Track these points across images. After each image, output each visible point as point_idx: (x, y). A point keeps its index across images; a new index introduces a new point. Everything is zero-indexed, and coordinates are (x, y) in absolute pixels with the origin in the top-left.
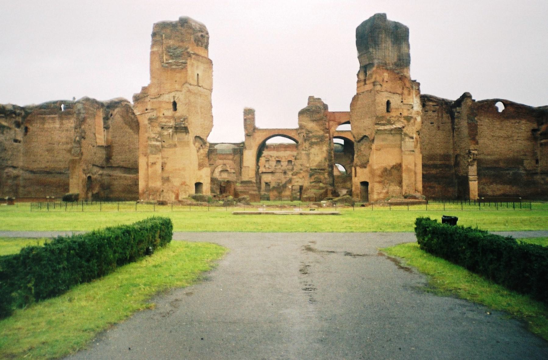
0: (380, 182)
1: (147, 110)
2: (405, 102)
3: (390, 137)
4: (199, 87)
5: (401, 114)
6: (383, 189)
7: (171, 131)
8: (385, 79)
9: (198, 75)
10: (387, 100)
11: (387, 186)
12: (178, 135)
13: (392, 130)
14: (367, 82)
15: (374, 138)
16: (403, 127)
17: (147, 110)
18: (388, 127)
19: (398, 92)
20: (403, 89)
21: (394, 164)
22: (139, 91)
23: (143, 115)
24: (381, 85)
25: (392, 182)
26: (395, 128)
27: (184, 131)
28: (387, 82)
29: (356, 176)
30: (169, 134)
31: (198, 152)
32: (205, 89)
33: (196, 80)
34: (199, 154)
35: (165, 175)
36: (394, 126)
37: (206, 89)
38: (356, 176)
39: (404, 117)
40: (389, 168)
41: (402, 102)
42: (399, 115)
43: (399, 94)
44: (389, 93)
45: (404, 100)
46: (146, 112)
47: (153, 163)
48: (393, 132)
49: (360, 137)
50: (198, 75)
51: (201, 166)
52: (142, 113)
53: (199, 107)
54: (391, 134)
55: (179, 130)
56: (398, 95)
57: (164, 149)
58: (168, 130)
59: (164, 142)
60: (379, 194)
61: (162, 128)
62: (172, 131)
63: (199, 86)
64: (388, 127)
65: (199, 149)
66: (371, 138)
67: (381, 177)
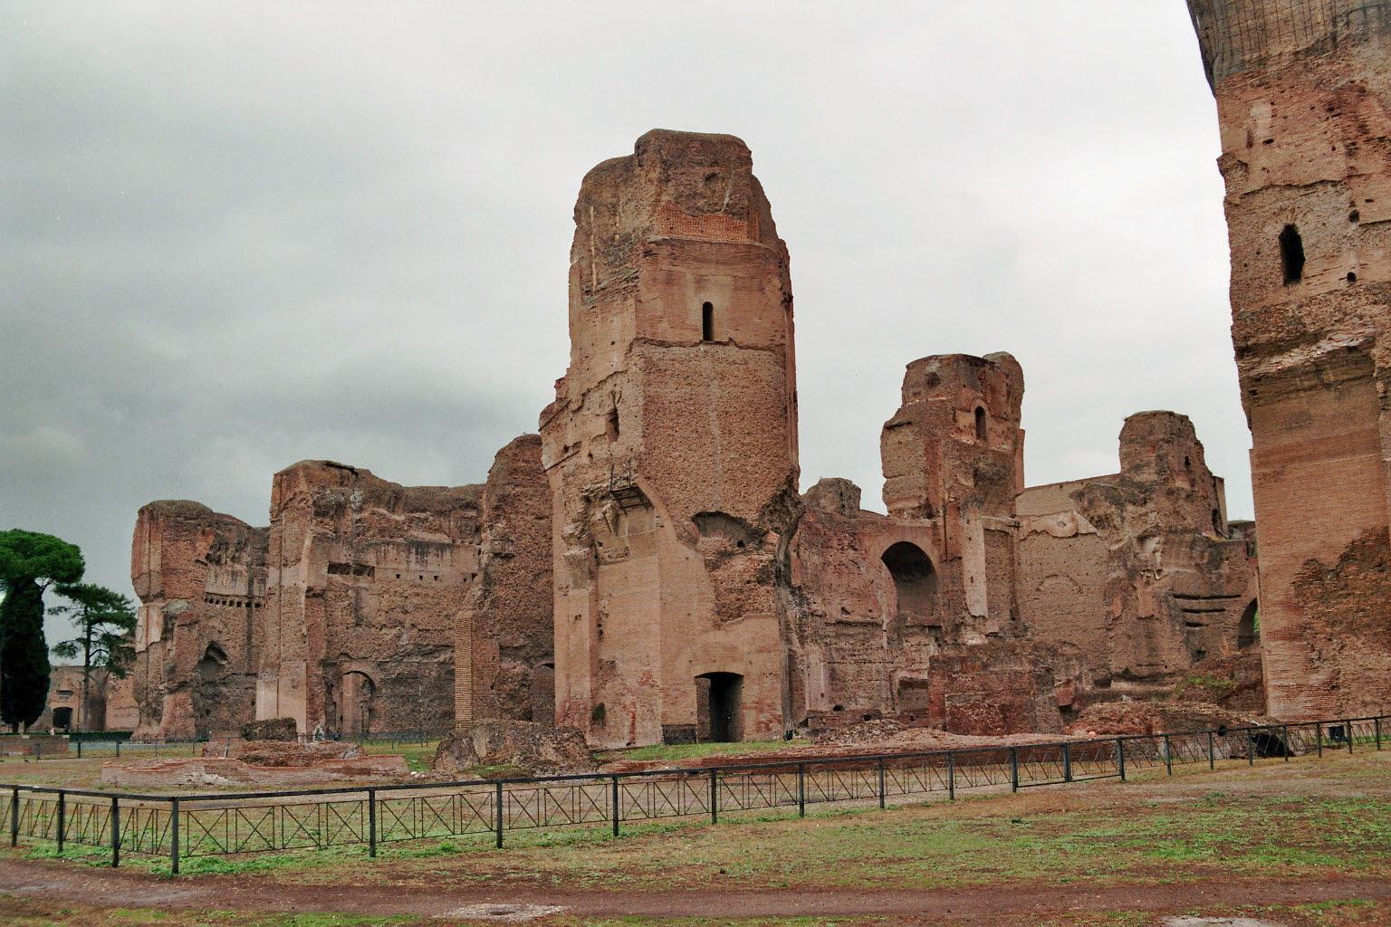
0: (1290, 636)
2: (1368, 214)
3: (1326, 404)
4: (719, 348)
5: (1351, 277)
6: (1310, 667)
7: (608, 504)
8: (1261, 133)
9: (707, 308)
10: (1280, 228)
11: (1330, 650)
12: (630, 514)
13: (1318, 367)
16: (1371, 342)
18: (1293, 359)
19: (1325, 177)
20: (1351, 152)
21: (1356, 534)
22: (551, 396)
24: (1246, 165)
25: (1353, 629)
26: (1332, 353)
27: (637, 501)
28: (1270, 142)
30: (605, 518)
31: (712, 566)
32: (748, 347)
33: (700, 324)
34: (719, 573)
35: (605, 657)
36: (1326, 346)
37: (755, 348)
39: (1367, 289)
40: (1330, 559)
41: (1354, 217)
42: (1344, 285)
43: (1334, 184)
44: (1287, 193)
45: (1361, 207)
46: (569, 454)
48: (1330, 376)
50: (707, 308)
51: (727, 613)
53: (713, 415)
54: (1328, 386)
56: (1330, 188)
57: (603, 568)
58: (603, 506)
59: (601, 544)
60: (1290, 693)
61: (587, 500)
62: (613, 507)
63: (719, 343)
64: (1293, 359)
65: (725, 555)
67: (1298, 609)
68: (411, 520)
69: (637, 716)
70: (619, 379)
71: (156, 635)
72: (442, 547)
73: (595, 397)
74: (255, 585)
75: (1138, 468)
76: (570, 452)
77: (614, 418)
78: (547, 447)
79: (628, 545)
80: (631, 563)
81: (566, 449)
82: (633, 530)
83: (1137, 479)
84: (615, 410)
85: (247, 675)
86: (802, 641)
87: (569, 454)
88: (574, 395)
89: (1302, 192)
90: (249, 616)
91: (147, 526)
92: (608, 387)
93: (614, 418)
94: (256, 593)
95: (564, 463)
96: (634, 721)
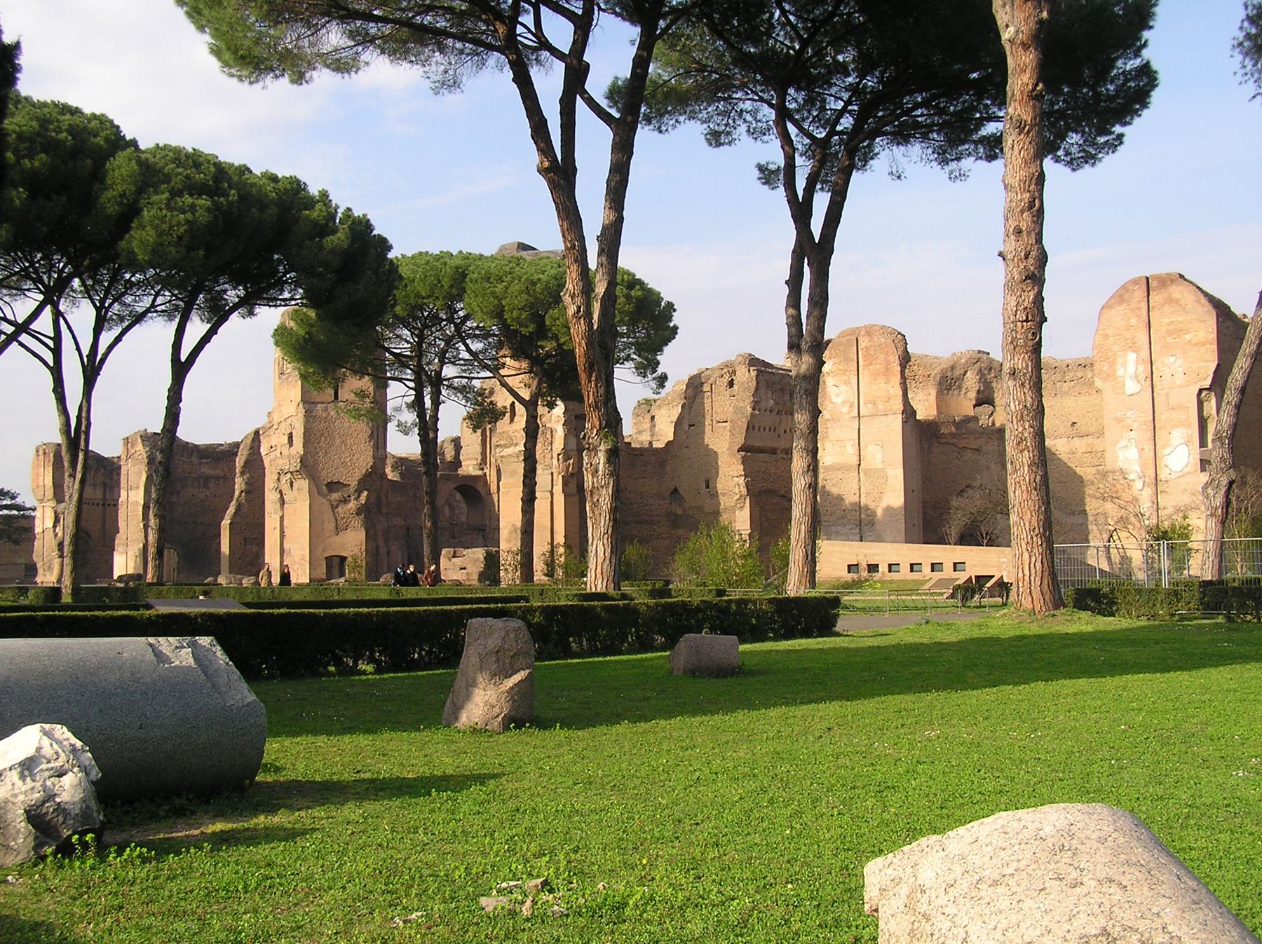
17: (272, 447)
68: (201, 464)
70: (293, 418)
71: (49, 523)
72: (218, 478)
73: (283, 425)
74: (108, 492)
75: (640, 432)
76: (274, 449)
77: (291, 436)
80: (298, 504)
81: (272, 447)
82: (298, 489)
83: (640, 439)
84: (291, 433)
85: (103, 546)
86: (387, 540)
88: (275, 422)
90: (104, 511)
91: (42, 458)
92: (289, 421)
93: (291, 436)
94: (108, 497)
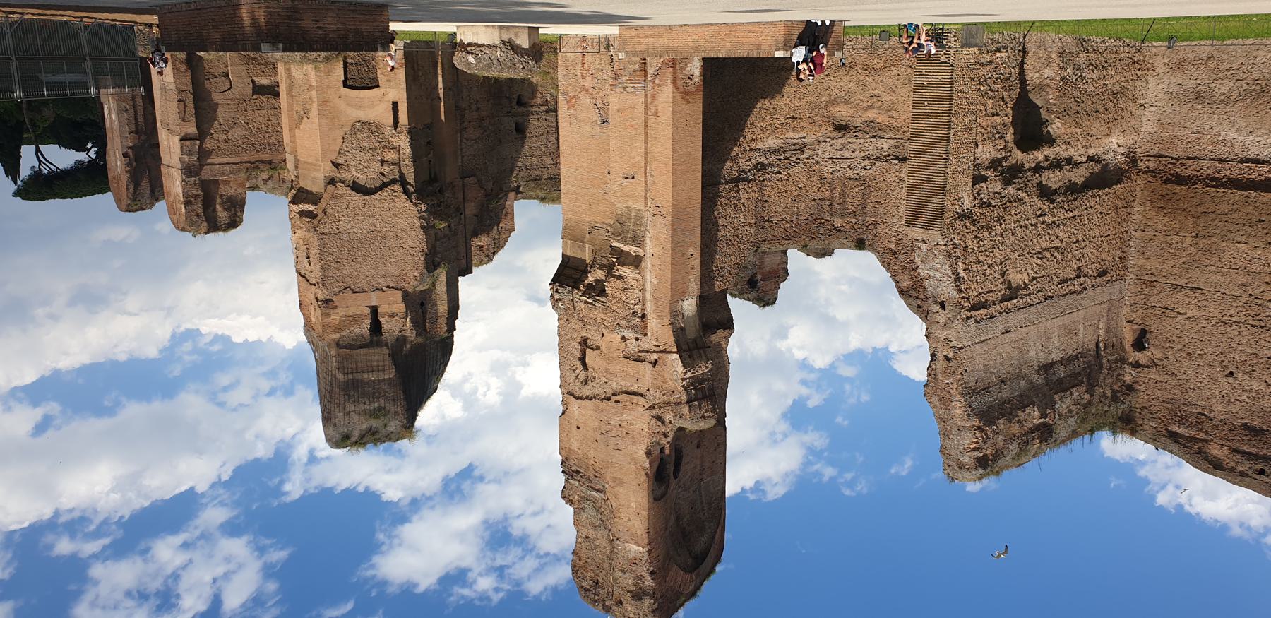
1: (654, 363)
7: (591, 278)
14: (368, 311)
15: (326, 187)
17: (654, 363)
23: (661, 348)
29: (395, 105)
38: (395, 105)
40: (305, 119)
46: (655, 356)
47: (633, 178)
49: (385, 194)
52: (665, 355)
55: (576, 275)
61: (602, 292)
66: (342, 190)
69: (580, 65)
78: (675, 377)
79: (588, 235)
87: (655, 356)
89: (307, 276)
92: (587, 391)
95: (657, 349)
96: (583, 60)
